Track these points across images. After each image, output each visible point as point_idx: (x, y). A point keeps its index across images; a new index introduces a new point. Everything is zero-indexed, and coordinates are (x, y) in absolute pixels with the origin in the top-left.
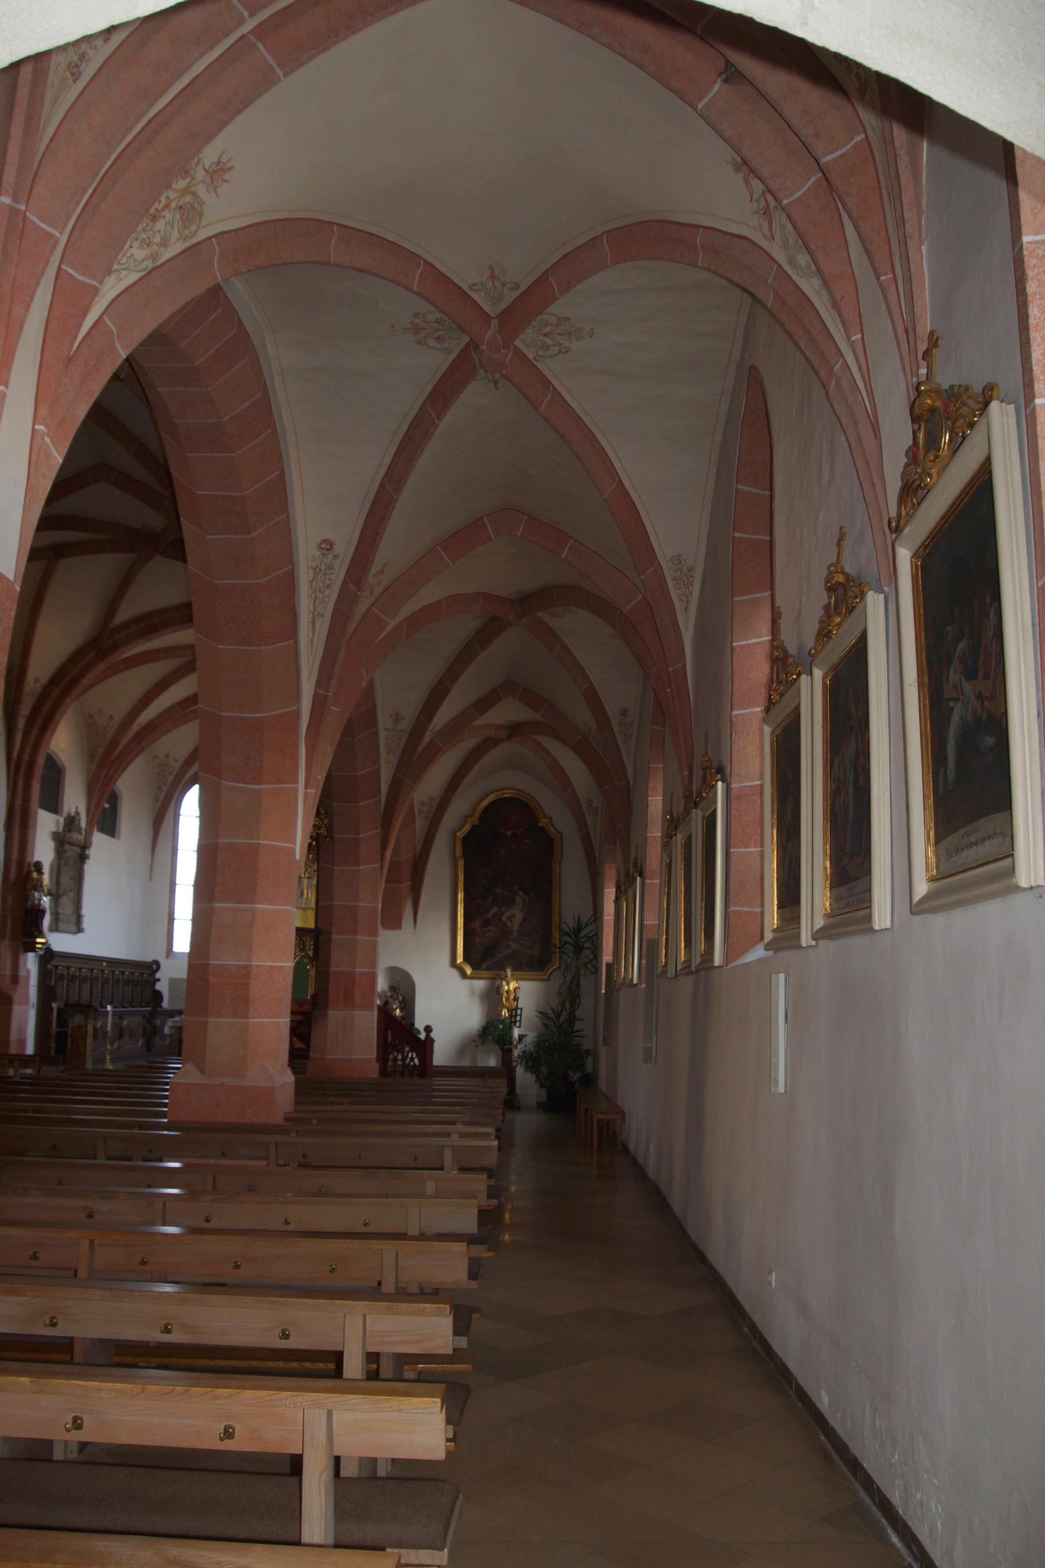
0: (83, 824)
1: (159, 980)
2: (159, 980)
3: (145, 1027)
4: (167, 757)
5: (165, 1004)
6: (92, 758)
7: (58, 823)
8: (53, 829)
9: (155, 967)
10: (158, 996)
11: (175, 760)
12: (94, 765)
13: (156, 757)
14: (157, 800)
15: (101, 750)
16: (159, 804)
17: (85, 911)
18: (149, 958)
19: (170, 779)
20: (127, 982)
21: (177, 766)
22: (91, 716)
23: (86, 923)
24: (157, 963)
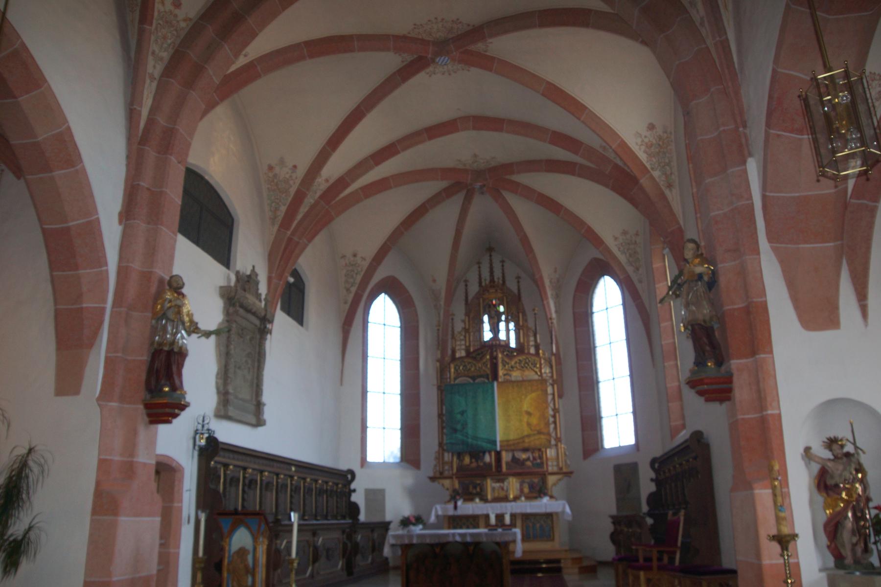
0: (263, 289)
1: (354, 491)
2: (354, 491)
3: (345, 544)
4: (355, 255)
5: (362, 517)
6: (273, 219)
7: (229, 279)
8: (223, 283)
9: (349, 476)
10: (354, 509)
11: (363, 259)
12: (276, 227)
13: (344, 257)
14: (346, 303)
15: (283, 209)
16: (347, 306)
17: (266, 398)
18: (343, 466)
19: (359, 278)
20: (320, 492)
21: (365, 264)
22: (271, 168)
23: (268, 413)
24: (352, 473)
